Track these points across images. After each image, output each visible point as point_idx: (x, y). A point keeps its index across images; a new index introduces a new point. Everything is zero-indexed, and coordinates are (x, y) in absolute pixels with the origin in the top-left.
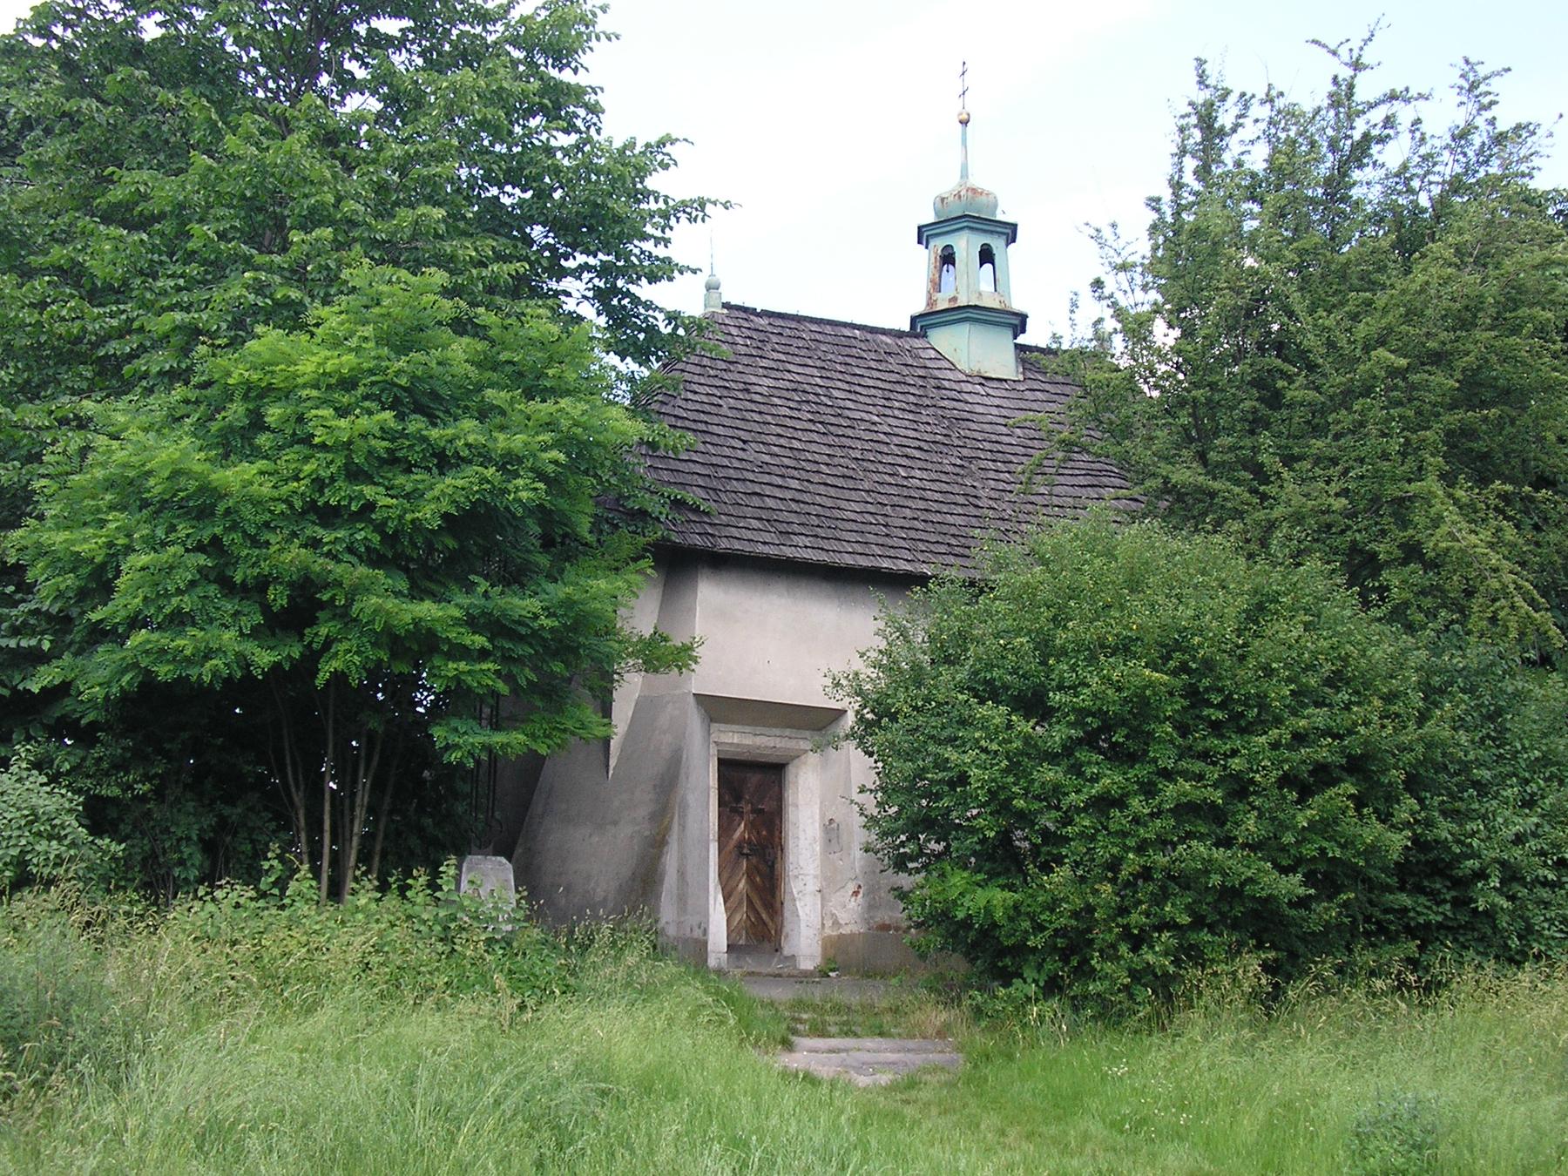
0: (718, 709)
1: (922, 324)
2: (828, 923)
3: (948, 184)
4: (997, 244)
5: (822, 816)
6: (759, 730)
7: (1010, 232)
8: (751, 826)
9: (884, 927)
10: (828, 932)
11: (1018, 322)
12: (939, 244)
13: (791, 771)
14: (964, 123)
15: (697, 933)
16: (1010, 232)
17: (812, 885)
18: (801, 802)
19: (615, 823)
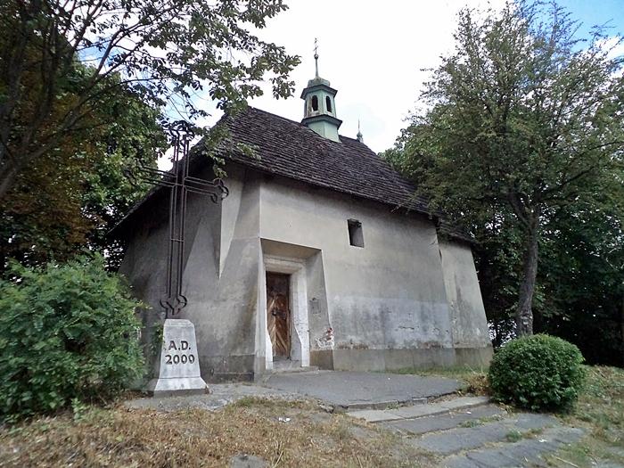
0: (269, 247)
1: (307, 121)
2: (313, 346)
3: (313, 77)
4: (331, 98)
5: (308, 298)
6: (283, 258)
7: (334, 92)
8: (277, 302)
9: (341, 347)
10: (313, 349)
11: (338, 123)
12: (311, 95)
13: (293, 279)
14: (316, 58)
15: (263, 355)
16: (334, 92)
17: (306, 328)
18: (299, 290)
19: (224, 300)
